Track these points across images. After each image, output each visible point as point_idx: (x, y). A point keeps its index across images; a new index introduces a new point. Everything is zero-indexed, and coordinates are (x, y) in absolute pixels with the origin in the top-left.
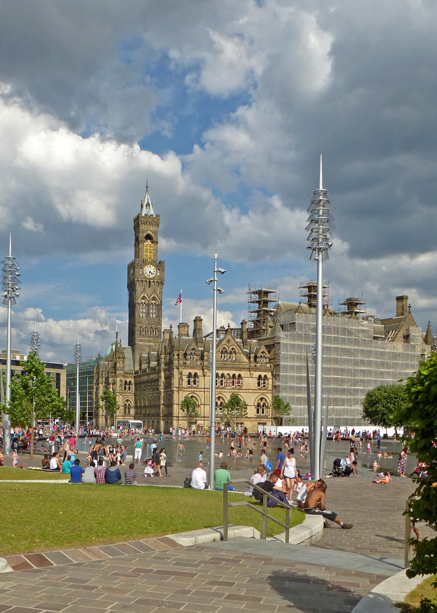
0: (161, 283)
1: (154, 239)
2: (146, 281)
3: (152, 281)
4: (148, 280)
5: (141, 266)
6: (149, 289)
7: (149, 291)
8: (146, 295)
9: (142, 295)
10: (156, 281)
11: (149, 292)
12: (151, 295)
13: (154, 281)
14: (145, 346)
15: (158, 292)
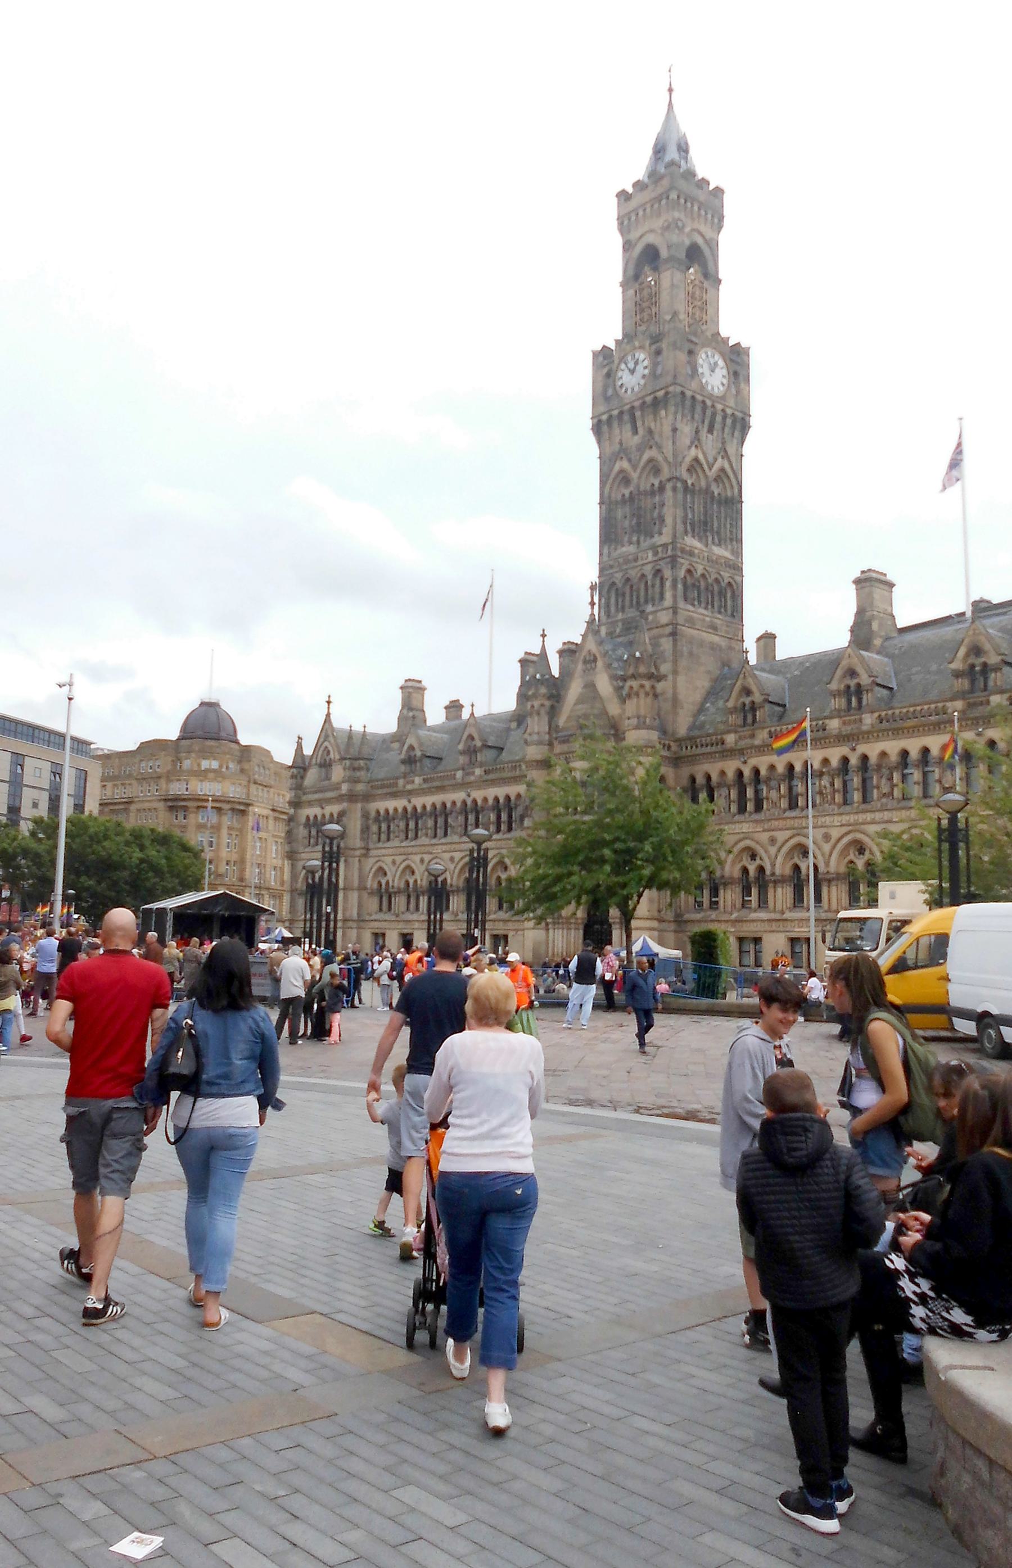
0: (741, 425)
1: (710, 264)
2: (703, 402)
3: (719, 407)
4: (709, 403)
5: (692, 346)
6: (709, 436)
7: (710, 442)
8: (701, 457)
9: (693, 452)
10: (729, 411)
11: (710, 443)
12: (716, 460)
13: (723, 410)
14: (701, 644)
15: (731, 450)
